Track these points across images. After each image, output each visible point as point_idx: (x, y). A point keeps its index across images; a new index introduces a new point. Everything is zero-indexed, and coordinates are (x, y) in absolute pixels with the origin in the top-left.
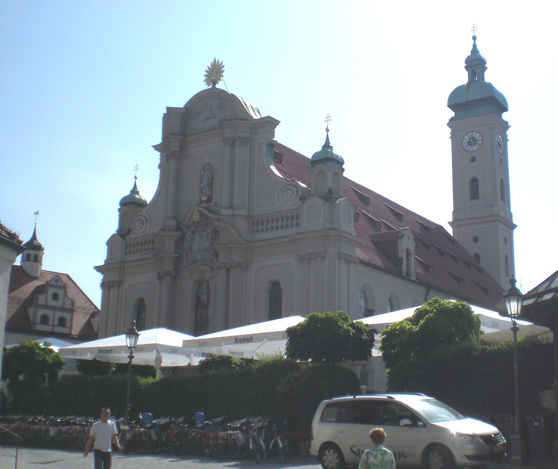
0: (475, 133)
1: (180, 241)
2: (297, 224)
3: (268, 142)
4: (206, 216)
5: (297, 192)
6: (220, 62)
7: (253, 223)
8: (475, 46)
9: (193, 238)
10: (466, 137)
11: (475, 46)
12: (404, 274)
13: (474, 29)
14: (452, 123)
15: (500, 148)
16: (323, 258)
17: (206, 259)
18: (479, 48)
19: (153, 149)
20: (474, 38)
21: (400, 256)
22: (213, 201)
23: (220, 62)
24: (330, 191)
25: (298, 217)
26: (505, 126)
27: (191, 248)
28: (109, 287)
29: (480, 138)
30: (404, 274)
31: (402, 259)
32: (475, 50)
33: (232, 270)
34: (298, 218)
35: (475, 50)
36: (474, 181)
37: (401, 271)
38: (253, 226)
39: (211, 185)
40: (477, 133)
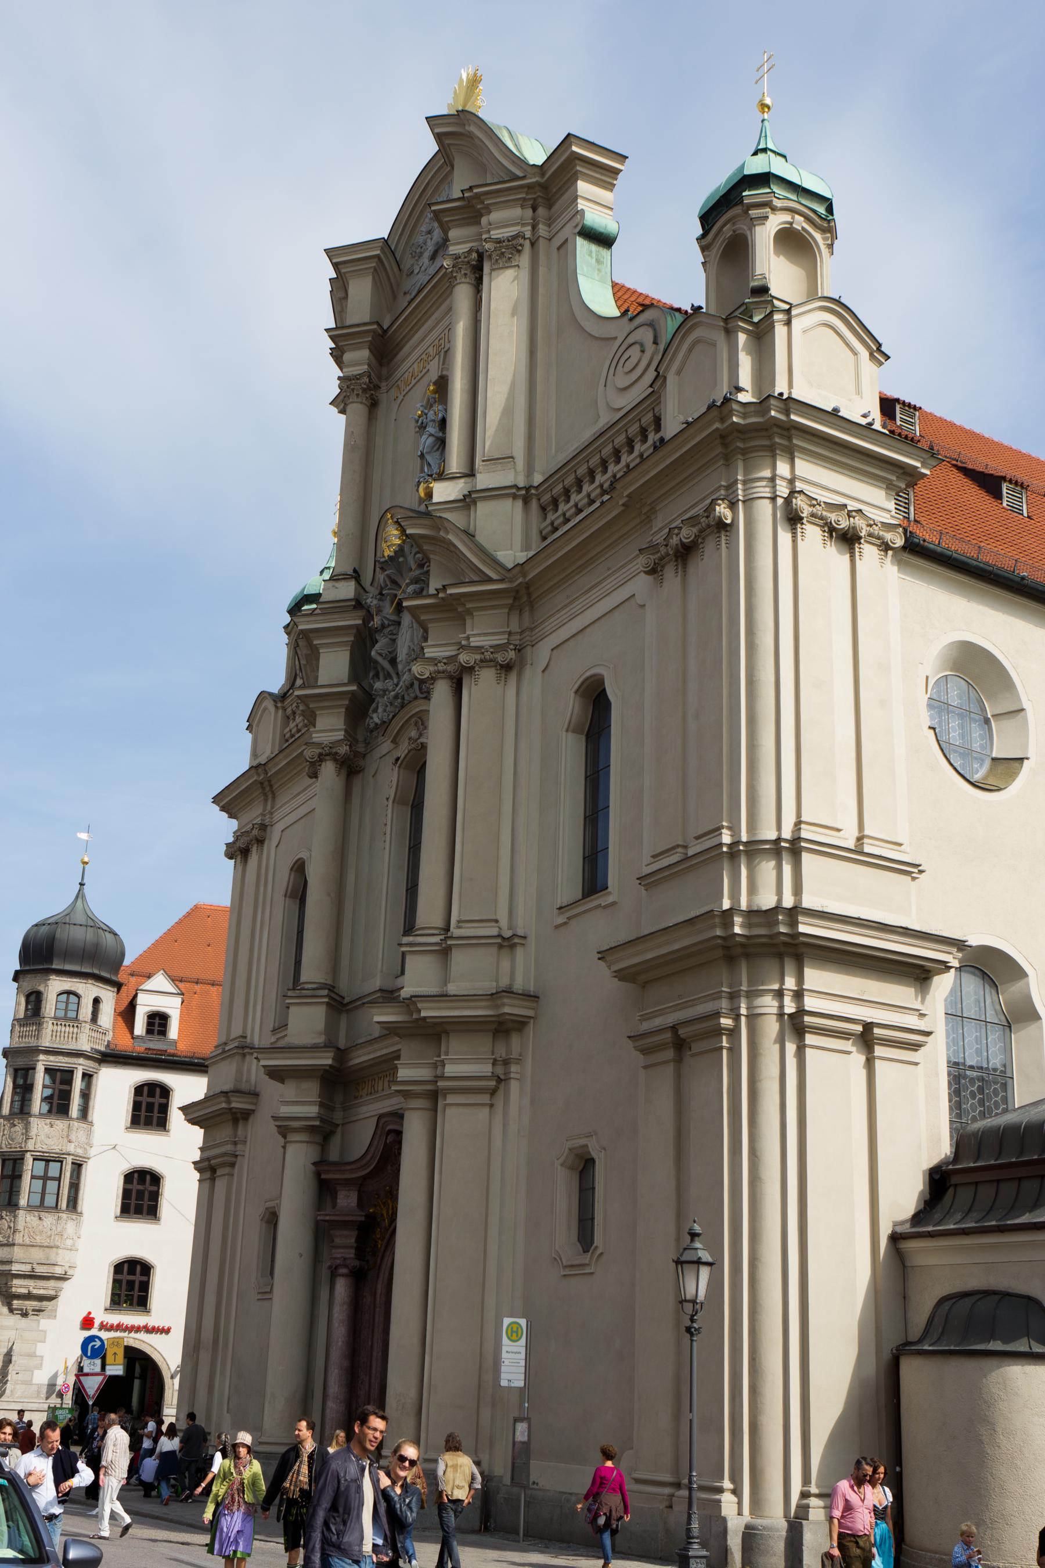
5: (655, 342)
27: (393, 661)
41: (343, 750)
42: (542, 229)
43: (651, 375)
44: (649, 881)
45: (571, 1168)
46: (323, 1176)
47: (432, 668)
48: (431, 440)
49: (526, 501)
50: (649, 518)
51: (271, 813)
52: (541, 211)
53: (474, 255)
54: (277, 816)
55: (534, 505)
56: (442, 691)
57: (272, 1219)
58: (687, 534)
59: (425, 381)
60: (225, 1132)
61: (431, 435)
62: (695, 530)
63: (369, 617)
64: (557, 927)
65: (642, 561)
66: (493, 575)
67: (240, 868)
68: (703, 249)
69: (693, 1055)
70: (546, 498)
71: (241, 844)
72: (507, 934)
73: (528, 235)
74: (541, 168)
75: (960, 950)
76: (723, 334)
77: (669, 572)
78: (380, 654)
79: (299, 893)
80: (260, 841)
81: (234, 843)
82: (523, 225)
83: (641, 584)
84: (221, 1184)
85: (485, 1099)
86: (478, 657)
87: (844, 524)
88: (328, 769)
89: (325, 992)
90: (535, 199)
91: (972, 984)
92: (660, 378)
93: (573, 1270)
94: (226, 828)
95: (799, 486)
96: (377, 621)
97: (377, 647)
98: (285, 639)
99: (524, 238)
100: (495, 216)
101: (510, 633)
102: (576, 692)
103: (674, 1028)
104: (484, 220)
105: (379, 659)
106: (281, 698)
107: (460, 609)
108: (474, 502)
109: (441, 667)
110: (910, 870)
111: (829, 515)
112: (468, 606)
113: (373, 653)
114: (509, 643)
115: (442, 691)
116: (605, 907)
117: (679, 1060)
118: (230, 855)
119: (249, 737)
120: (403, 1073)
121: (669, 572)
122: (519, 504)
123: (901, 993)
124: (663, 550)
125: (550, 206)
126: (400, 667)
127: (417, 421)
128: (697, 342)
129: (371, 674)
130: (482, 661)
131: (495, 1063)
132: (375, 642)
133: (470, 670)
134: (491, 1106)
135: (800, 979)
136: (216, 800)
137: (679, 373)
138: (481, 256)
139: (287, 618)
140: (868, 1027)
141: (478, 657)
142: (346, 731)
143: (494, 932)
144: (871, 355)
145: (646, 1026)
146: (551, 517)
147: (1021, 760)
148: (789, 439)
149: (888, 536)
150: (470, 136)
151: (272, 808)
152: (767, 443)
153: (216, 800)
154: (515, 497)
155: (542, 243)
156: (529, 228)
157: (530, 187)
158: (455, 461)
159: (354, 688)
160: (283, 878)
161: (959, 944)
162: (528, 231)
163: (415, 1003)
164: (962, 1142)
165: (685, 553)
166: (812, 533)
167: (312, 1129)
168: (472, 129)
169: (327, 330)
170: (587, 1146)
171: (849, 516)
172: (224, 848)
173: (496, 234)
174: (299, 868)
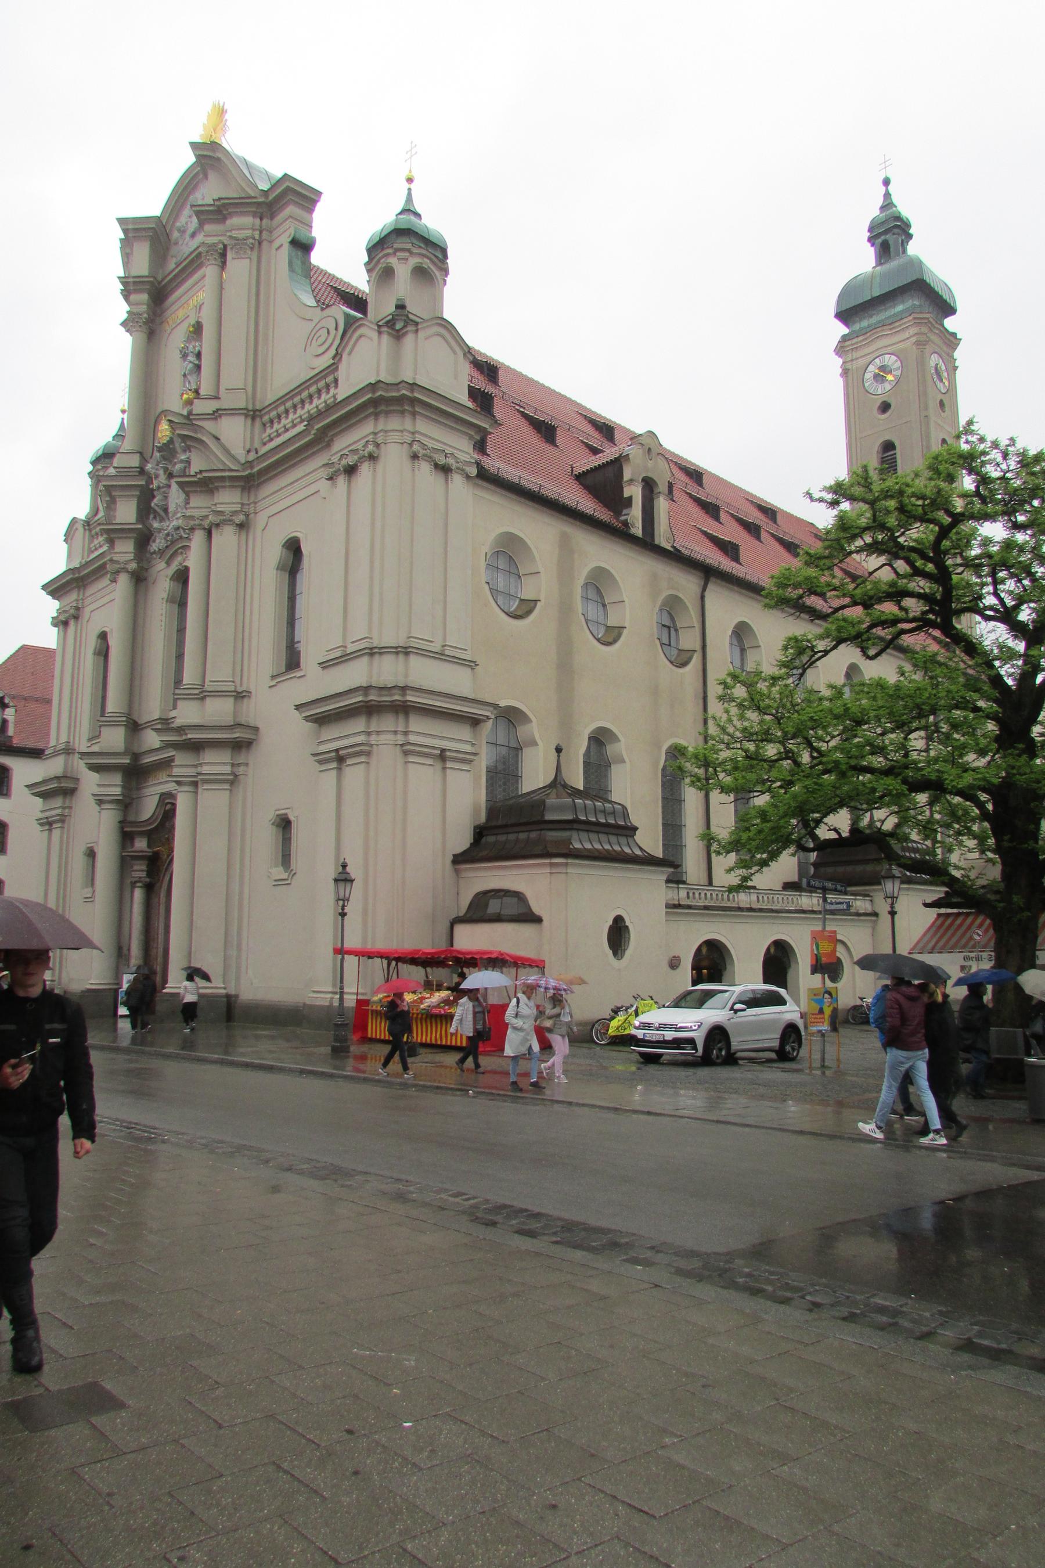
0: (887, 357)
1: (145, 496)
3: (290, 239)
6: (221, 105)
7: (264, 425)
8: (887, 195)
10: (871, 368)
11: (887, 195)
12: (637, 530)
13: (886, 163)
14: (841, 349)
15: (941, 380)
16: (372, 458)
18: (895, 199)
20: (886, 182)
21: (626, 494)
23: (221, 105)
24: (400, 307)
26: (952, 341)
28: (65, 624)
29: (898, 364)
30: (637, 530)
31: (630, 499)
32: (888, 204)
33: (214, 532)
34: (336, 387)
35: (888, 204)
36: (888, 446)
37: (626, 524)
38: (265, 430)
40: (893, 356)
41: (133, 566)
42: (265, 235)
43: (332, 352)
44: (325, 665)
45: (278, 826)
46: (125, 829)
47: (192, 523)
48: (191, 365)
49: (253, 419)
50: (328, 445)
51: (83, 599)
52: (265, 221)
54: (87, 601)
55: (258, 420)
56: (198, 537)
57: (91, 854)
58: (351, 460)
59: (185, 325)
60: (58, 802)
61: (191, 362)
62: (356, 457)
63: (150, 480)
64: (270, 687)
65: (324, 473)
66: (234, 468)
67: (62, 633)
68: (369, 271)
69: (347, 766)
70: (266, 418)
71: (63, 618)
72: (240, 690)
73: (257, 237)
74: (265, 193)
75: (495, 709)
76: (377, 334)
77: (341, 480)
79: (103, 652)
80: (76, 617)
81: (57, 617)
82: (254, 230)
83: (324, 485)
84: (56, 834)
85: (227, 786)
86: (222, 518)
87: (442, 460)
88: (123, 579)
89: (124, 719)
91: (502, 725)
92: (337, 355)
93: (280, 883)
94: (52, 606)
95: (418, 437)
96: (155, 485)
97: (155, 501)
98: (89, 481)
99: (254, 238)
100: (235, 221)
101: (243, 504)
102: (283, 546)
103: (337, 751)
104: (228, 222)
105: (156, 508)
106: (88, 524)
107: (211, 486)
108: (220, 416)
109: (197, 522)
110: (471, 665)
111: (435, 456)
112: (216, 484)
113: (152, 505)
114: (241, 511)
115: (198, 537)
116: (299, 677)
117: (339, 769)
118: (55, 625)
119: (65, 546)
120: (176, 771)
121: (341, 480)
122: (249, 421)
123: (464, 732)
124: (337, 466)
125: (272, 218)
126: (170, 515)
127: (181, 352)
128: (361, 336)
129: (152, 516)
131: (233, 765)
132: (154, 497)
133: (218, 525)
134: (231, 790)
135: (407, 726)
136: (44, 587)
137: (350, 354)
138: (225, 247)
139: (90, 468)
140: (443, 751)
141: (222, 518)
142: (135, 553)
143: (232, 688)
144: (465, 355)
145: (323, 748)
146: (269, 431)
147: (536, 601)
148: (413, 407)
149: (468, 469)
150: (219, 159)
151: (84, 595)
152: (399, 408)
153: (44, 587)
154: (246, 416)
155: (265, 244)
156: (258, 232)
157: (259, 204)
159: (140, 526)
160: (91, 643)
161: (496, 706)
162: (257, 235)
163: (184, 730)
164: (492, 811)
165: (351, 470)
166: (425, 467)
167: (118, 801)
168: (220, 155)
169: (119, 278)
170: (286, 814)
171: (446, 456)
172: (51, 620)
173: (234, 234)
174: (103, 636)
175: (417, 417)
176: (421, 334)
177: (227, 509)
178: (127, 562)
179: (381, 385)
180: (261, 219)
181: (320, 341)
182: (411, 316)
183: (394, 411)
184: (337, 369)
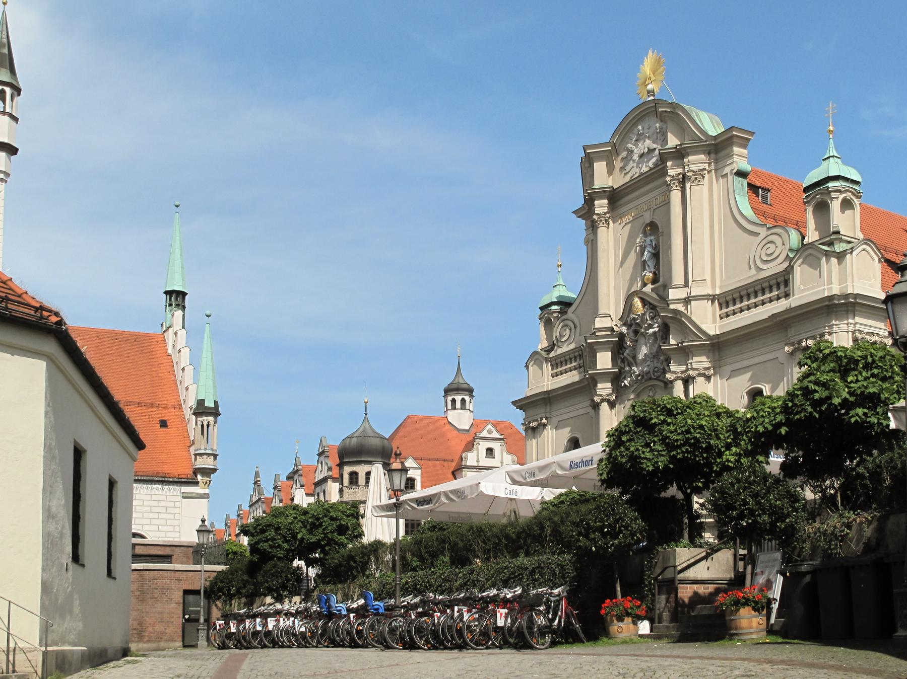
2: (787, 295)
4: (650, 304)
9: (637, 341)
17: (656, 369)
19: (574, 215)
22: (661, 279)
25: (786, 282)
39: (656, 255)
47: (674, 375)
53: (681, 176)
61: (649, 252)
74: (715, 138)
78: (629, 355)
86: (697, 372)
90: (710, 150)
95: (858, 327)
100: (690, 158)
104: (686, 160)
105: (628, 357)
109: (679, 375)
122: (710, 302)
130: (698, 374)
141: (697, 372)
148: (854, 307)
152: (846, 309)
154: (708, 299)
158: (678, 277)
173: (692, 167)
175: (856, 313)
176: (854, 253)
177: (701, 366)
178: (608, 395)
179: (836, 297)
180: (709, 154)
181: (769, 252)
182: (843, 237)
183: (841, 311)
184: (789, 274)
